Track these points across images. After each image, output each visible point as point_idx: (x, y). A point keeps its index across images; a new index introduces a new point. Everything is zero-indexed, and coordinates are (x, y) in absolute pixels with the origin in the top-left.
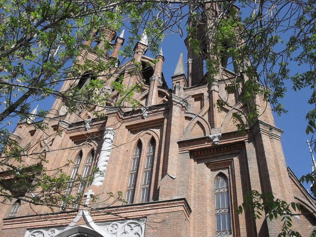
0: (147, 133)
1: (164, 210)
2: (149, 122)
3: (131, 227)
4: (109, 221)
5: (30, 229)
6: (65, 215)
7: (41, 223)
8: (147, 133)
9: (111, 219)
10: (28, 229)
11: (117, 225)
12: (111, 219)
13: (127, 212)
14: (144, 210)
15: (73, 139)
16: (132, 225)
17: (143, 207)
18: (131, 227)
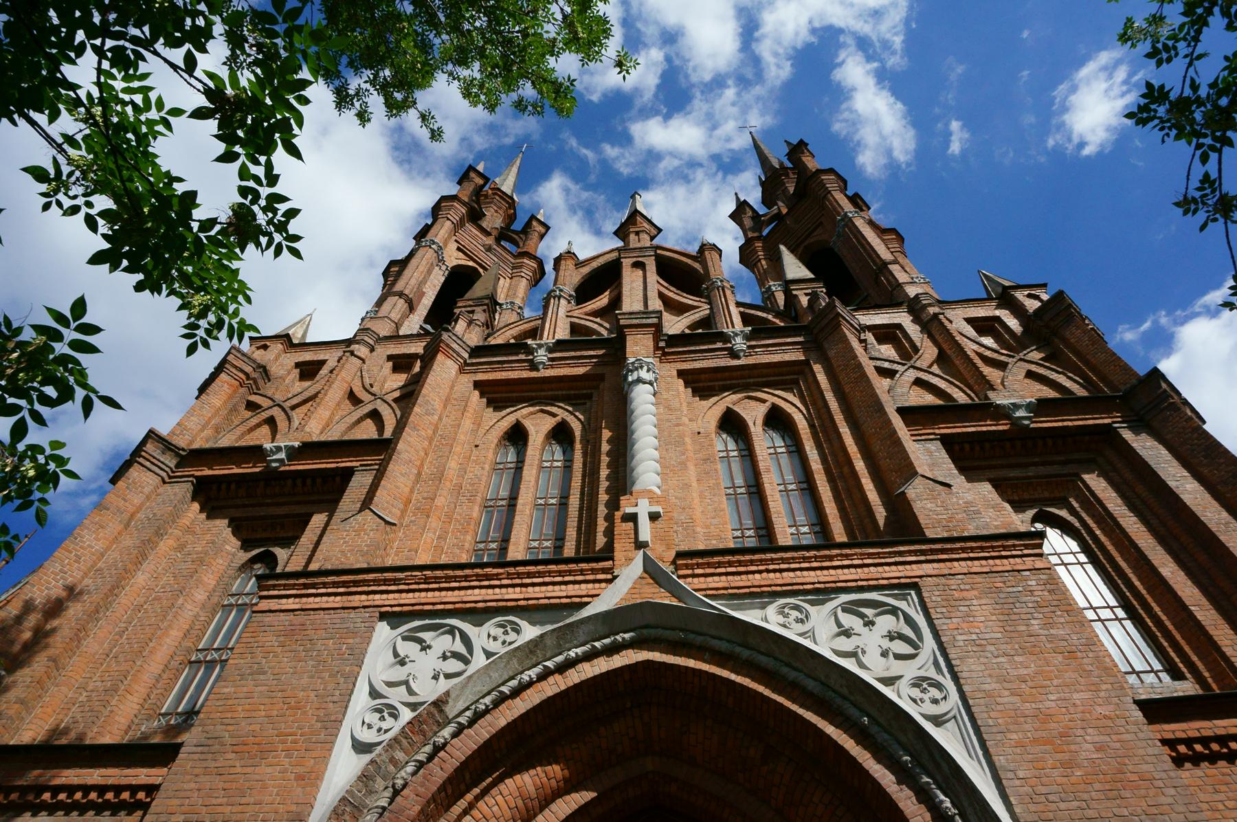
1: (976, 566)
2: (755, 366)
3: (862, 616)
5: (393, 618)
9: (770, 586)
10: (383, 616)
11: (797, 608)
12: (770, 586)
13: (827, 568)
16: (869, 612)
17: (890, 553)
18: (862, 616)
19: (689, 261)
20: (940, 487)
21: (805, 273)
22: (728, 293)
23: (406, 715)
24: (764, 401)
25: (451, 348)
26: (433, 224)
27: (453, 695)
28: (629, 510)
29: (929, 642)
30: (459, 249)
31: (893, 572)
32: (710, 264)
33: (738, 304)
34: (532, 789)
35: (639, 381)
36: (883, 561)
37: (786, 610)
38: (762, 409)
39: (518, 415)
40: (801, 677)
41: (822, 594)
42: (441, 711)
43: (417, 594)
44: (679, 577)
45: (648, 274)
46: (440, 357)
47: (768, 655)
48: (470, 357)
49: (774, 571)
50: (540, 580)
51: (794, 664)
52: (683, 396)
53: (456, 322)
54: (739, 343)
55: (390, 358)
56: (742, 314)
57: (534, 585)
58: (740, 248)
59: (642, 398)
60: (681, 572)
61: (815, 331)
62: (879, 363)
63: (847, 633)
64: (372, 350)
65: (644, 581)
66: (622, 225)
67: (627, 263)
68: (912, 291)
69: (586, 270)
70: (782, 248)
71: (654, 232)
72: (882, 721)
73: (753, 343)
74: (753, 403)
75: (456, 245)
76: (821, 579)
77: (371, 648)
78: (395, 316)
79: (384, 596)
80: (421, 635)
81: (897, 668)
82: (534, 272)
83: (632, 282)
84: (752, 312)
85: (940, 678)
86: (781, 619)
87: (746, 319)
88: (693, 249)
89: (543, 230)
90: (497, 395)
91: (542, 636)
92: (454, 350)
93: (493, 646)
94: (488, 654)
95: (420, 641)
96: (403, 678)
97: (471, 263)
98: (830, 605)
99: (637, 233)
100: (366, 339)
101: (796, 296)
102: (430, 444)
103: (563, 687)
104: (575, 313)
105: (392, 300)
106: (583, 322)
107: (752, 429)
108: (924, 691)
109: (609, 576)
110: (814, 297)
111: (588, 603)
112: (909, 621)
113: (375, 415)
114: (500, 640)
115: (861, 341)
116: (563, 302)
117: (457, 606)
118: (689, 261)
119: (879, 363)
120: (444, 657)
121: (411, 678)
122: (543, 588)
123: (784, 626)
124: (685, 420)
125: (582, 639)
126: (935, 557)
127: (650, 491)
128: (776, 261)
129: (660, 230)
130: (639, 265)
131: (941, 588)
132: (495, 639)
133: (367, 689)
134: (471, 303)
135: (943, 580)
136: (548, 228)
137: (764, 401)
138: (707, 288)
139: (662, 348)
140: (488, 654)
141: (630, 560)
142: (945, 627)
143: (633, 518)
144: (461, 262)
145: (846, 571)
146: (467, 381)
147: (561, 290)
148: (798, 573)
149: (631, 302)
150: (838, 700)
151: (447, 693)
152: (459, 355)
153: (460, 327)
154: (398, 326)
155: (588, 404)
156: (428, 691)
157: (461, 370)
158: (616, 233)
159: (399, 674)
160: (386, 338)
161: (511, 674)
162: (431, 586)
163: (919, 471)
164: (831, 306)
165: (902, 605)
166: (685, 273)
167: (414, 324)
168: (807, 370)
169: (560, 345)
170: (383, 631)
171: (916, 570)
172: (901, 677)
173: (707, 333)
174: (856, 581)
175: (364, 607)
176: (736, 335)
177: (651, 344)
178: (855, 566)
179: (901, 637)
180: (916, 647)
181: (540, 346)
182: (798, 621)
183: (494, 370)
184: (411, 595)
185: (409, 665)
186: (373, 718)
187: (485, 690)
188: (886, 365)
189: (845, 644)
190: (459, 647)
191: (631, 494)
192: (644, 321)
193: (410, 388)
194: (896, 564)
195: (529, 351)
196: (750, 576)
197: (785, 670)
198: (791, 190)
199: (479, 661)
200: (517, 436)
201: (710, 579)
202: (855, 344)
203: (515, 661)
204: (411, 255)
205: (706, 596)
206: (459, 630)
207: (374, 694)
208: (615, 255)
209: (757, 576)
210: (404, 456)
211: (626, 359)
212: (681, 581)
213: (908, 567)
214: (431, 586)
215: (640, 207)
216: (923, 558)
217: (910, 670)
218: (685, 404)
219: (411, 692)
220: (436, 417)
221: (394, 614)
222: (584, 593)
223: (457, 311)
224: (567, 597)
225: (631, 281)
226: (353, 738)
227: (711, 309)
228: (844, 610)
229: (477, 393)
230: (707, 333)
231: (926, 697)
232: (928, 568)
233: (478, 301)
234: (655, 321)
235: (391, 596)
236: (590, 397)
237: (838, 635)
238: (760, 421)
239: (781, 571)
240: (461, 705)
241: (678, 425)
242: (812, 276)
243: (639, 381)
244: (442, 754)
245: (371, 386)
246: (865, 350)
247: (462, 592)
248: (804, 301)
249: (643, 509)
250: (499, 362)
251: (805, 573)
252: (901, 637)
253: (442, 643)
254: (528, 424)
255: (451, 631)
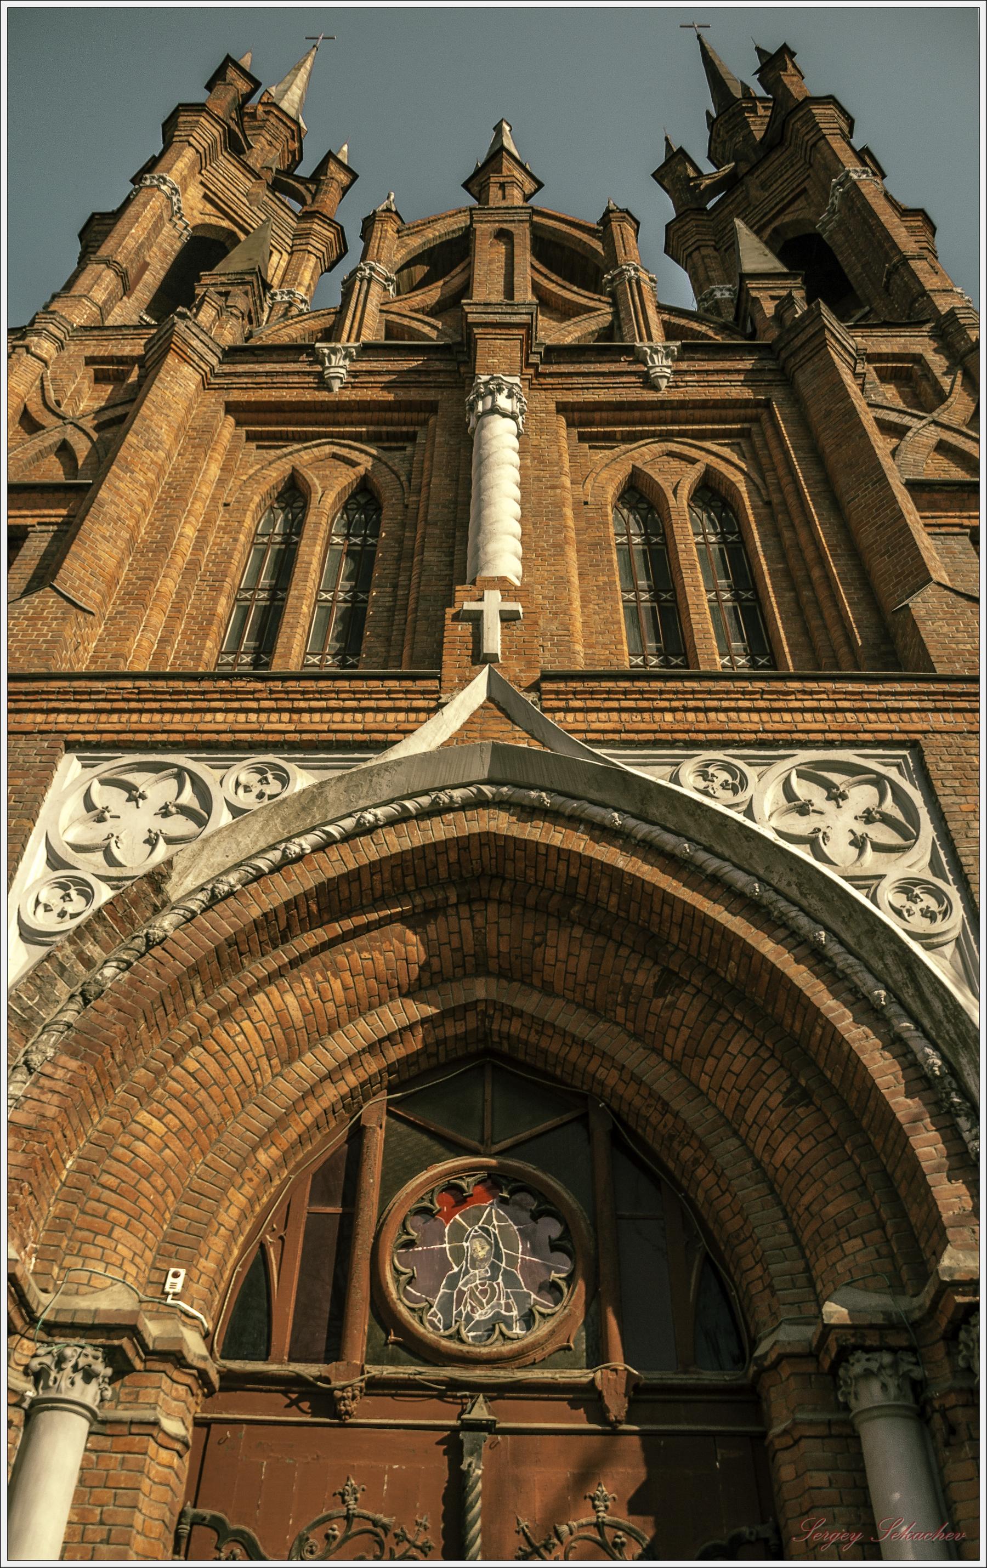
0: (671, 454)
2: (682, 405)
3: (828, 786)
4: (672, 744)
5: (89, 748)
6: (354, 692)
7: (178, 722)
8: (671, 454)
9: (687, 731)
11: (727, 767)
12: (687, 731)
14: (886, 710)
15: (243, 416)
17: (880, 693)
18: (828, 786)
19: (585, 237)
20: (964, 603)
21: (772, 264)
22: (646, 288)
23: (104, 894)
24: (693, 461)
25: (190, 346)
26: (163, 154)
27: (178, 867)
28: (469, 606)
29: (928, 831)
30: (206, 197)
31: (879, 722)
32: (619, 243)
33: (661, 308)
34: (296, 1014)
35: (495, 410)
36: (868, 705)
37: (711, 770)
38: (690, 477)
39: (295, 460)
40: (727, 868)
41: (770, 745)
42: (158, 890)
43: (125, 717)
44: (545, 710)
45: (517, 251)
46: (171, 360)
47: (677, 834)
48: (221, 362)
49: (696, 710)
50: (323, 704)
51: (719, 849)
52: (564, 444)
53: (199, 308)
54: (661, 366)
55: (90, 361)
56: (666, 325)
57: (311, 710)
58: (668, 227)
59: (502, 439)
60: (548, 704)
61: (783, 355)
62: (882, 414)
63: (803, 809)
64: (61, 347)
65: (488, 713)
66: (478, 171)
67: (484, 229)
68: (943, 304)
69: (415, 242)
70: (738, 222)
71: (529, 186)
72: (847, 937)
73: (684, 366)
74: (675, 463)
75: (202, 190)
76: (768, 726)
77: (50, 795)
78: (100, 295)
79: (73, 718)
80: (130, 777)
81: (871, 861)
82: (329, 246)
83: (491, 262)
84: (683, 322)
85: (940, 883)
86: (702, 784)
87: (671, 332)
88: (592, 218)
89: (343, 178)
90: (264, 423)
91: (322, 785)
92: (194, 350)
93: (244, 800)
94: (236, 811)
95: (129, 788)
96: (99, 840)
97: (225, 224)
98: (781, 768)
99: (502, 186)
100: (51, 327)
101: (756, 300)
102: (151, 494)
103: (352, 866)
104: (395, 307)
105: (93, 269)
106: (406, 322)
107: (672, 502)
108: (913, 898)
109: (433, 704)
110: (786, 303)
111: (395, 742)
112: (901, 798)
113: (64, 449)
114: (256, 791)
115: (856, 375)
116: (375, 289)
117: (189, 737)
118: (585, 237)
119: (882, 414)
120: (165, 812)
121: (113, 840)
122: (327, 717)
123: (705, 793)
124: (567, 482)
125: (386, 794)
126: (950, 705)
127: (504, 580)
128: (730, 247)
129: (540, 185)
130: (504, 235)
131: (955, 750)
132: (247, 789)
133: (42, 854)
134: (223, 279)
135: (958, 739)
136: (354, 177)
137: (693, 461)
138: (611, 281)
139: (535, 366)
140: (236, 811)
141: (465, 682)
142: (955, 808)
143: (476, 619)
144: (208, 220)
145: (808, 716)
146: (214, 400)
147: (372, 269)
148: (733, 715)
149: (487, 288)
150: (782, 904)
151: (169, 863)
152: (202, 358)
153: (207, 315)
154: (104, 311)
155: (409, 450)
156: (136, 860)
157: (205, 384)
158: (466, 185)
159: (93, 833)
160: (84, 328)
161: (271, 840)
162: (148, 705)
163: (933, 575)
164: (813, 315)
165: (893, 773)
166: (576, 258)
167: (129, 311)
168: (765, 416)
169: (367, 349)
170: (70, 769)
171: (917, 722)
172: (881, 877)
173: (611, 345)
174: (823, 732)
175: (41, 732)
176: (656, 352)
177: (517, 355)
178: (824, 711)
179: (887, 820)
180: (906, 835)
181: (334, 351)
182: (725, 785)
183: (259, 386)
184: (115, 718)
185: (110, 822)
186: (51, 896)
187: (230, 862)
188: (893, 417)
189: (801, 826)
190: (188, 797)
191: (473, 583)
192: (507, 319)
193: (120, 411)
194: (886, 710)
195: (318, 359)
196: (657, 716)
197: (702, 856)
198: (759, 135)
199: (222, 817)
200: (293, 494)
201: (592, 716)
202: (848, 378)
203: (278, 821)
204: (128, 202)
205: (586, 741)
206: (190, 773)
207: (55, 861)
208: (462, 221)
209: (669, 717)
210: (110, 510)
211: (474, 376)
212: (548, 716)
213: (905, 716)
214: (148, 705)
215: (508, 143)
216: (930, 705)
217: (897, 869)
218: (566, 457)
219: (112, 861)
220: (162, 454)
221: (88, 746)
222: (392, 727)
223: (200, 291)
224: (364, 732)
225: (488, 260)
226: (20, 922)
227: (616, 314)
228: (800, 775)
229: (231, 420)
230: (611, 345)
231: (916, 908)
232: (937, 721)
233: (240, 280)
234: (526, 318)
235: (84, 718)
236: (411, 437)
237: (788, 811)
238: (685, 492)
239: (707, 710)
240: (190, 883)
241: (554, 487)
242: (785, 270)
243: (495, 410)
244: (157, 952)
245: (58, 404)
246: (862, 391)
247: (197, 717)
248: (769, 308)
249: (492, 604)
250: (268, 374)
251: (744, 716)
252: (887, 820)
253: (159, 790)
254: (313, 479)
255: (180, 774)
